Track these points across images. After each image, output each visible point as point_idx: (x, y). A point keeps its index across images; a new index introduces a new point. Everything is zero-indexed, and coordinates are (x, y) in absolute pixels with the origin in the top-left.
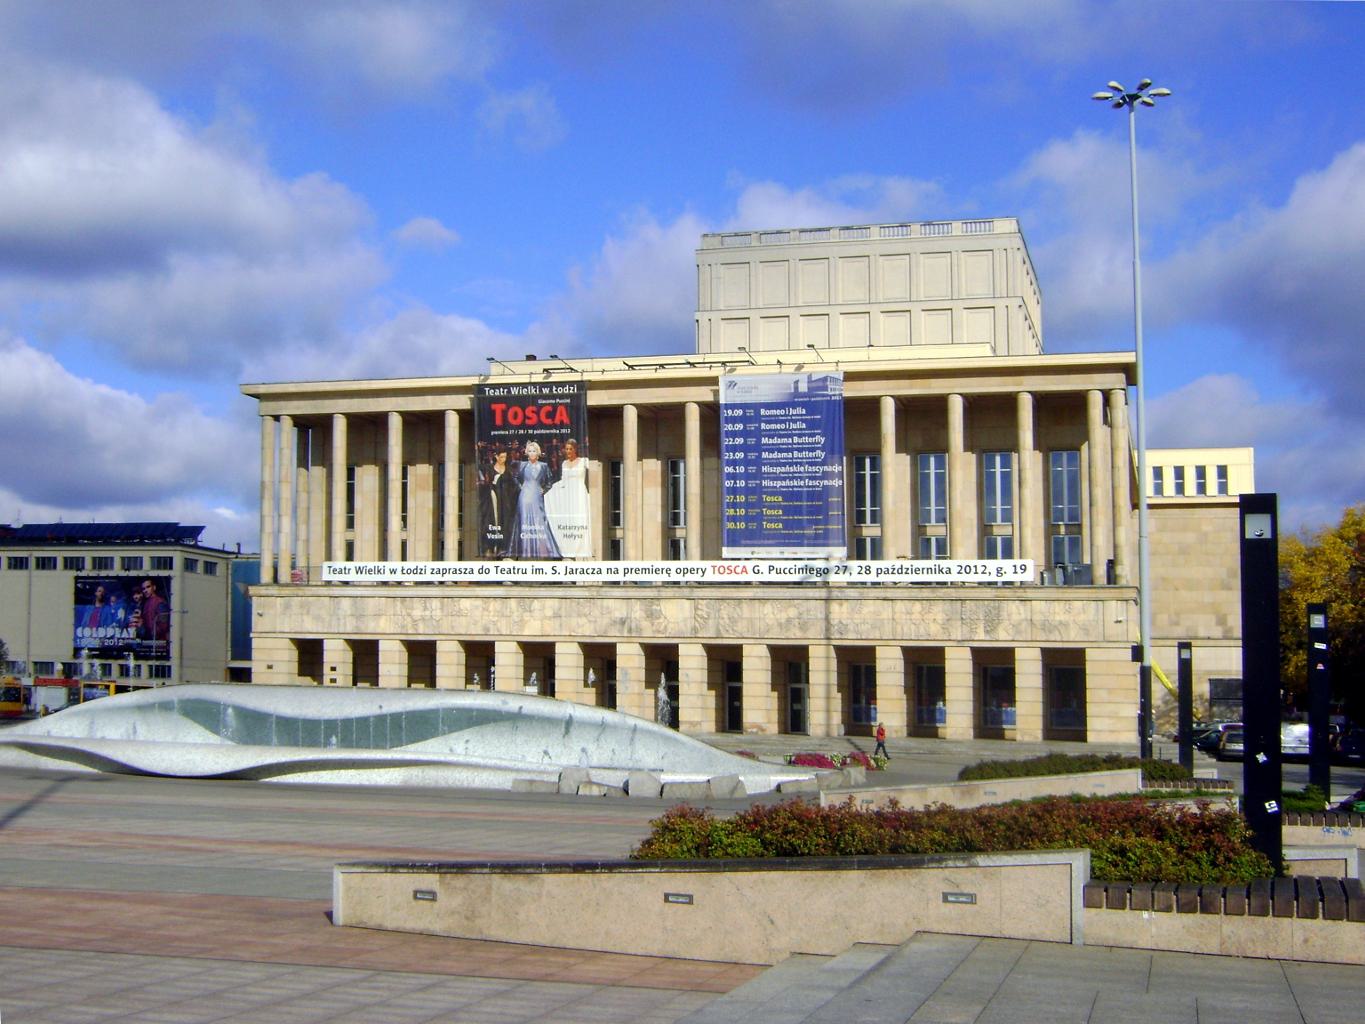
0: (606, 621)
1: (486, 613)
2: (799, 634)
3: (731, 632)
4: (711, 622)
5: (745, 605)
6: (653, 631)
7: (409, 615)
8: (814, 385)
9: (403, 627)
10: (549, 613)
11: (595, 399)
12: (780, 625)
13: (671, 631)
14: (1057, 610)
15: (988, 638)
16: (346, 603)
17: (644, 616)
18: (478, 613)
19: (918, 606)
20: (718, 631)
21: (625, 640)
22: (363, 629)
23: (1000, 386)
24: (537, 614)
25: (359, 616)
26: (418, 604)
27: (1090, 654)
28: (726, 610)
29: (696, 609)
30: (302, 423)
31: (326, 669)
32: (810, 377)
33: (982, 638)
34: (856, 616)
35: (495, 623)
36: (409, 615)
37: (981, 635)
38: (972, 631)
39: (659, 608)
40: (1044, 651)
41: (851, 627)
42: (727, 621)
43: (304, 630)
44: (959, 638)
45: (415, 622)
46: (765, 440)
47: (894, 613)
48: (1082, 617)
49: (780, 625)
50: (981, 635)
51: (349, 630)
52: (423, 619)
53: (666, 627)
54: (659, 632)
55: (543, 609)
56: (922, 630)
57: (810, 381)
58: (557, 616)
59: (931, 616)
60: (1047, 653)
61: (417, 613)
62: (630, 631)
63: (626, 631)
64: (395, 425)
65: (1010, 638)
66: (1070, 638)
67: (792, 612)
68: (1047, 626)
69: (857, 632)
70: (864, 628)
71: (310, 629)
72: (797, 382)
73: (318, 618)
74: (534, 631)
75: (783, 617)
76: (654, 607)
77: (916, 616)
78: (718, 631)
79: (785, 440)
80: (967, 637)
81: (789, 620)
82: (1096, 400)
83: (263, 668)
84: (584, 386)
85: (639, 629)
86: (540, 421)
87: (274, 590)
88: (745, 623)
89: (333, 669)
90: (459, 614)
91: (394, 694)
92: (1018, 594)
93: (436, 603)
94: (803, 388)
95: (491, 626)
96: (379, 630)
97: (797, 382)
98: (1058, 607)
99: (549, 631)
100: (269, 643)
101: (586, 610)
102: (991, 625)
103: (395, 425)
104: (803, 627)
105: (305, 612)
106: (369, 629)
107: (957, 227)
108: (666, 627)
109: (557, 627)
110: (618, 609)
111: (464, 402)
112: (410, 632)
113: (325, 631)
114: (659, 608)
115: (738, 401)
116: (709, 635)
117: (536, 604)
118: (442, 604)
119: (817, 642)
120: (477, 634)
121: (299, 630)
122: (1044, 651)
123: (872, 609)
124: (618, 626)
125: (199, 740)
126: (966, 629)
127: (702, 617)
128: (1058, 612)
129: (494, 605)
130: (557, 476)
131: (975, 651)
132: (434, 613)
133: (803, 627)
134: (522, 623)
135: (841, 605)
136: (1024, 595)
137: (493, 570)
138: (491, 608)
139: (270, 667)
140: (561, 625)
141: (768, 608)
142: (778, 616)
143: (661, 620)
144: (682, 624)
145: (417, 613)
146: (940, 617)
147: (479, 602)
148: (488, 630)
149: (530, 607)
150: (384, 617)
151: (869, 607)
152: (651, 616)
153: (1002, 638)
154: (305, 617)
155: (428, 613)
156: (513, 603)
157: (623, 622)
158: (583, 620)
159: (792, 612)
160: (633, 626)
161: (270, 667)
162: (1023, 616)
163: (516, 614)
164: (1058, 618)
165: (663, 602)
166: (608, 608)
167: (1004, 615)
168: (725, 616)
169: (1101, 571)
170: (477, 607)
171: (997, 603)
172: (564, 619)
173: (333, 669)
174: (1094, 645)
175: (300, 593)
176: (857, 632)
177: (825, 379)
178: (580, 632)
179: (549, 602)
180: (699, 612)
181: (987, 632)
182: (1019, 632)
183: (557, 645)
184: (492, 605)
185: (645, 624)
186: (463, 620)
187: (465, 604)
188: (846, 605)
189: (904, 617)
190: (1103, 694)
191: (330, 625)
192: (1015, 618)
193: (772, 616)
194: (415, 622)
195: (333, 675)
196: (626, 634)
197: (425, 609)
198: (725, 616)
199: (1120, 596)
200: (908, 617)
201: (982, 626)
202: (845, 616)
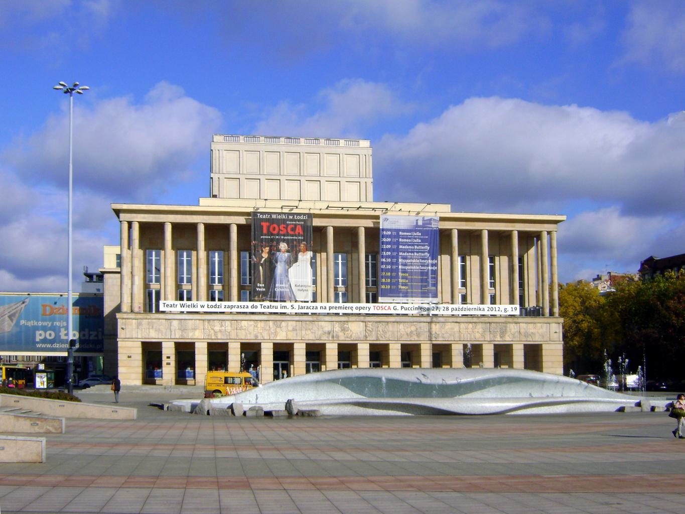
0: (320, 332)
1: (256, 328)
3: (384, 337)
4: (374, 333)
5: (390, 325)
6: (345, 338)
7: (213, 329)
8: (426, 222)
10: (290, 328)
11: (317, 222)
12: (407, 334)
13: (354, 337)
14: (530, 327)
16: (175, 324)
17: (340, 330)
18: (251, 328)
19: (471, 325)
20: (377, 337)
21: (331, 342)
22: (185, 336)
23: (505, 227)
24: (284, 329)
25: (183, 329)
27: (544, 347)
28: (381, 327)
29: (366, 326)
30: (145, 228)
31: (164, 358)
32: (423, 218)
33: (499, 340)
34: (442, 330)
35: (261, 334)
36: (213, 329)
37: (499, 339)
39: (348, 326)
40: (525, 346)
41: (440, 335)
42: (382, 332)
43: (150, 337)
44: (489, 340)
45: (216, 333)
46: (401, 247)
47: (459, 327)
48: (541, 331)
49: (407, 334)
50: (499, 339)
51: (177, 336)
52: (220, 331)
53: (351, 336)
54: (347, 337)
55: (287, 326)
56: (472, 337)
57: (423, 220)
58: (294, 330)
59: (476, 330)
60: (210, 345)
61: (217, 328)
62: (333, 337)
63: (331, 337)
64: (168, 230)
65: (511, 340)
66: (535, 340)
67: (413, 328)
68: (527, 335)
69: (443, 337)
70: (446, 335)
71: (153, 336)
72: (417, 220)
73: (158, 330)
75: (409, 330)
76: (345, 326)
77: (470, 330)
78: (377, 337)
79: (410, 247)
80: (493, 340)
81: (411, 332)
82: (545, 237)
83: (125, 357)
84: (311, 216)
85: (338, 336)
86: (287, 232)
87: (132, 316)
88: (390, 333)
89: (168, 357)
91: (488, 368)
92: (515, 320)
93: (228, 323)
94: (420, 223)
95: (259, 335)
96: (195, 337)
97: (417, 220)
98: (531, 326)
99: (290, 337)
100: (129, 344)
101: (310, 327)
102: (503, 333)
103: (168, 230)
104: (418, 335)
105: (151, 327)
106: (188, 337)
107: (342, 142)
108: (351, 336)
109: (295, 335)
110: (327, 327)
111: (242, 220)
112: (213, 338)
113: (163, 337)
114: (348, 326)
115: (389, 227)
116: (373, 339)
117: (284, 324)
118: (231, 324)
119: (298, 341)
120: (250, 338)
121: (147, 337)
122: (525, 346)
123: (449, 327)
124: (327, 335)
125: (494, 396)
126: (492, 336)
127: (370, 331)
128: (531, 328)
129: (260, 324)
130: (296, 260)
131: (495, 346)
132: (227, 328)
133: (418, 335)
134: (276, 333)
135: (436, 325)
136: (517, 321)
137: (259, 306)
138: (259, 326)
139: (129, 357)
140: (297, 334)
141: (401, 326)
142: (406, 330)
143: (349, 332)
144: (359, 334)
145: (217, 327)
146: (481, 330)
147: (252, 323)
148: (256, 336)
149: (280, 326)
150: (198, 330)
152: (343, 330)
153: (507, 340)
154: (151, 330)
155: (223, 328)
156: (271, 323)
157: (329, 333)
158: (308, 332)
159: (413, 328)
161: (129, 357)
162: (516, 330)
163: (272, 329)
164: (531, 331)
165: (349, 323)
166: (321, 326)
167: (508, 329)
168: (381, 330)
169: (547, 311)
170: (251, 325)
171: (505, 325)
172: (298, 331)
173: (168, 357)
174: (546, 343)
175: (148, 317)
176: (443, 337)
177: (430, 220)
178: (307, 337)
179: (290, 323)
180: (368, 328)
181: (501, 337)
182: (514, 337)
183: (295, 344)
184: (259, 324)
185: (341, 334)
186: (243, 332)
187: (244, 323)
188: (438, 325)
189: (464, 330)
190: (550, 364)
191: (166, 335)
193: (403, 330)
194: (216, 333)
195: (168, 361)
196: (330, 339)
197: (222, 326)
198: (381, 330)
199: (556, 321)
200: (466, 330)
201: (499, 335)
202: (438, 330)
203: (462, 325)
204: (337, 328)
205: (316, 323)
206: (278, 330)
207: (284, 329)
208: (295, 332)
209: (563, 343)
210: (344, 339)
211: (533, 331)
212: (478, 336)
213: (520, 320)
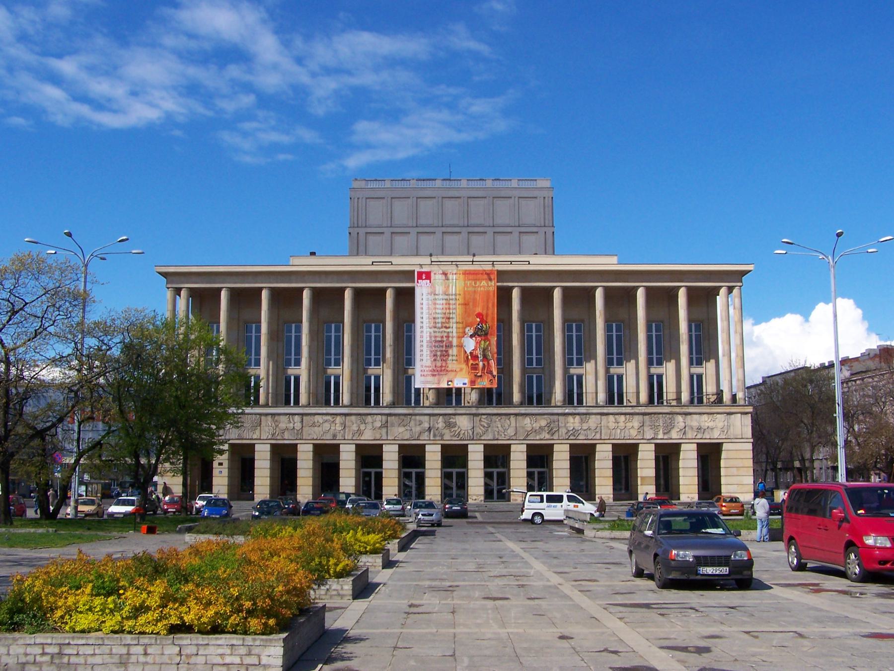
0: (418, 429)
2: (547, 436)
9: (273, 435)
10: (378, 424)
15: (666, 437)
19: (622, 418)
24: (370, 426)
26: (284, 419)
27: (725, 446)
33: (662, 438)
37: (660, 436)
38: (656, 434)
52: (287, 429)
59: (629, 425)
62: (435, 436)
66: (715, 436)
67: (543, 423)
74: (368, 437)
90: (314, 425)
93: (297, 418)
104: (551, 432)
116: (489, 438)
117: (369, 419)
124: (427, 433)
128: (705, 421)
134: (360, 432)
141: (527, 420)
145: (283, 425)
151: (593, 421)
152: (449, 425)
153: (675, 436)
155: (292, 425)
156: (353, 418)
159: (543, 423)
160: (437, 432)
164: (707, 424)
165: (457, 417)
181: (664, 434)
185: (446, 431)
187: (317, 418)
188: (577, 417)
192: (682, 425)
203: (611, 418)
204: (440, 423)
205: (413, 417)
206: (362, 427)
207: (370, 426)
208: (384, 430)
209: (752, 440)
210: (449, 439)
211: (711, 424)
212: (634, 433)
213: (691, 410)
